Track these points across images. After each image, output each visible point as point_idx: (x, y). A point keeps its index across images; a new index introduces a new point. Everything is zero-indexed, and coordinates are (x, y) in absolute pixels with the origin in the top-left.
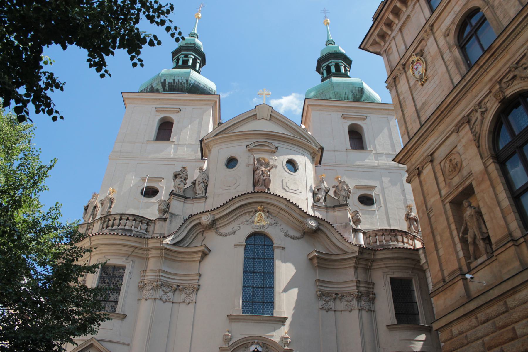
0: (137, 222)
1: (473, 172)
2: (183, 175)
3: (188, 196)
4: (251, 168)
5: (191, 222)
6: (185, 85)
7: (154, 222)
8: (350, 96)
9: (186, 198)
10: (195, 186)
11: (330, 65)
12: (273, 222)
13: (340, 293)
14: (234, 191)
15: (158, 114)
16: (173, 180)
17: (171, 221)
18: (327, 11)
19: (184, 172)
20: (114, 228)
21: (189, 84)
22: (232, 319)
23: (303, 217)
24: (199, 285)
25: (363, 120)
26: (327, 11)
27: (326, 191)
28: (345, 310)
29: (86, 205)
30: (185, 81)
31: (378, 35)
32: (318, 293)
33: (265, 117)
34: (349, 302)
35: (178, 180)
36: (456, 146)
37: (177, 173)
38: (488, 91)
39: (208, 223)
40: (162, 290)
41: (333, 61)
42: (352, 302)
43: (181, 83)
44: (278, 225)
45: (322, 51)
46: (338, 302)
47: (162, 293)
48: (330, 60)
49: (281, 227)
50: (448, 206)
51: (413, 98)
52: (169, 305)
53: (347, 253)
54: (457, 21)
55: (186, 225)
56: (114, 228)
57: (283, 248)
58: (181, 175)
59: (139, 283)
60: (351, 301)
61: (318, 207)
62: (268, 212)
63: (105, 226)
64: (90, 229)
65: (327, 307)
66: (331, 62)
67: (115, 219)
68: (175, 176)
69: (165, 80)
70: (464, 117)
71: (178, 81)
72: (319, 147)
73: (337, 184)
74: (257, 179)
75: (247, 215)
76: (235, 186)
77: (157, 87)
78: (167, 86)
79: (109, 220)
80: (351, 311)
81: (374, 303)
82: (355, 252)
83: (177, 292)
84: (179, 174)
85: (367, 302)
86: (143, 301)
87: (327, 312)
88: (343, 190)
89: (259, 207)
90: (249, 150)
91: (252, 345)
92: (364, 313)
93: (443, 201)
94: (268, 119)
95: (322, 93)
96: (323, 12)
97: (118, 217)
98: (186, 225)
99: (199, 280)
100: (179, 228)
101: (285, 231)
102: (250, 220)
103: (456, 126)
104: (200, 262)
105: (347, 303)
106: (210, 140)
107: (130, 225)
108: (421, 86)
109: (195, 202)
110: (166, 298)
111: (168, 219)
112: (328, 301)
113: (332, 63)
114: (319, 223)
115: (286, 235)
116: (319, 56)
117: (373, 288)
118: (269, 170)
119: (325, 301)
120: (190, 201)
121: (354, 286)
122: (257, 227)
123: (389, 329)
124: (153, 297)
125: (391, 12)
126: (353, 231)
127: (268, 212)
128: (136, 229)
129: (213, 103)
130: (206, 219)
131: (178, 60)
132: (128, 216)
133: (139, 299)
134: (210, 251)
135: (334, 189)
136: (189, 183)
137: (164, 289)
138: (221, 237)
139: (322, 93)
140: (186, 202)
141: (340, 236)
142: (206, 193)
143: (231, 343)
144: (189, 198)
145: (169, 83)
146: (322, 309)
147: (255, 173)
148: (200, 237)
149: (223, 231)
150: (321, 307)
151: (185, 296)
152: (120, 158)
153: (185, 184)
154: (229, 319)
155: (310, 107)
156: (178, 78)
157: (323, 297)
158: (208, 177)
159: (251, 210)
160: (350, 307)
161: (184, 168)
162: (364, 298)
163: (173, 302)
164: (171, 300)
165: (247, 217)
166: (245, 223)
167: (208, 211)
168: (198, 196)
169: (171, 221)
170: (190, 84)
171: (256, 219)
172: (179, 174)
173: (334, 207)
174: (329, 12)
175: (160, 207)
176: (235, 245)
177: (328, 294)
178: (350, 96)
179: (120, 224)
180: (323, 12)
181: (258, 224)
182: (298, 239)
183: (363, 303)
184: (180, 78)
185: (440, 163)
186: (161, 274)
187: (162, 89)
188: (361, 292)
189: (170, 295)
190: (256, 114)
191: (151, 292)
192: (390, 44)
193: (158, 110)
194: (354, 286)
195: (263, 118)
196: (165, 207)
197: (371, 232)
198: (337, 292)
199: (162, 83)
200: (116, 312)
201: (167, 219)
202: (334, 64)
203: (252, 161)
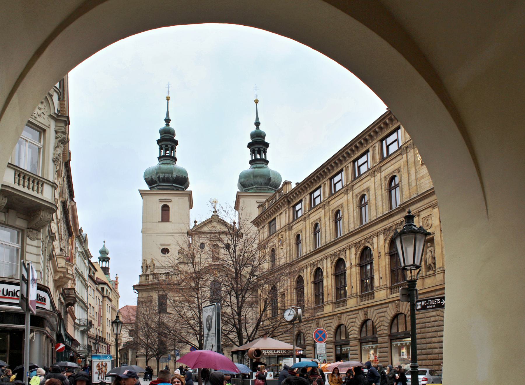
6: (171, 179)
8: (263, 183)
11: (255, 149)
15: (161, 203)
41: (257, 146)
43: (169, 178)
69: (159, 176)
77: (155, 179)
78: (161, 179)
113: (256, 147)
178: (263, 183)
193: (161, 201)
202: (257, 149)
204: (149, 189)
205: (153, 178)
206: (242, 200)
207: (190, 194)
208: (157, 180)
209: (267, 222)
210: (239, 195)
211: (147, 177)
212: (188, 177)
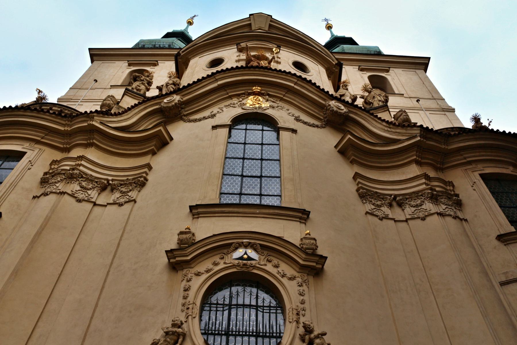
22: (198, 214)
23: (324, 100)
25: (386, 72)
39: (173, 104)
42: (423, 207)
44: (284, 109)
47: (78, 188)
48: (338, 45)
49: (289, 112)
60: (421, 205)
85: (449, 206)
89: (254, 88)
91: (236, 249)
98: (137, 110)
99: (147, 174)
102: (239, 103)
112: (380, 206)
119: (373, 204)
123: (502, 242)
133: (34, 197)
134: (172, 139)
141: (384, 124)
146: (372, 214)
156: (159, 43)
163: (95, 204)
164: (93, 200)
166: (231, 105)
183: (444, 207)
186: (83, 162)
191: (57, 185)
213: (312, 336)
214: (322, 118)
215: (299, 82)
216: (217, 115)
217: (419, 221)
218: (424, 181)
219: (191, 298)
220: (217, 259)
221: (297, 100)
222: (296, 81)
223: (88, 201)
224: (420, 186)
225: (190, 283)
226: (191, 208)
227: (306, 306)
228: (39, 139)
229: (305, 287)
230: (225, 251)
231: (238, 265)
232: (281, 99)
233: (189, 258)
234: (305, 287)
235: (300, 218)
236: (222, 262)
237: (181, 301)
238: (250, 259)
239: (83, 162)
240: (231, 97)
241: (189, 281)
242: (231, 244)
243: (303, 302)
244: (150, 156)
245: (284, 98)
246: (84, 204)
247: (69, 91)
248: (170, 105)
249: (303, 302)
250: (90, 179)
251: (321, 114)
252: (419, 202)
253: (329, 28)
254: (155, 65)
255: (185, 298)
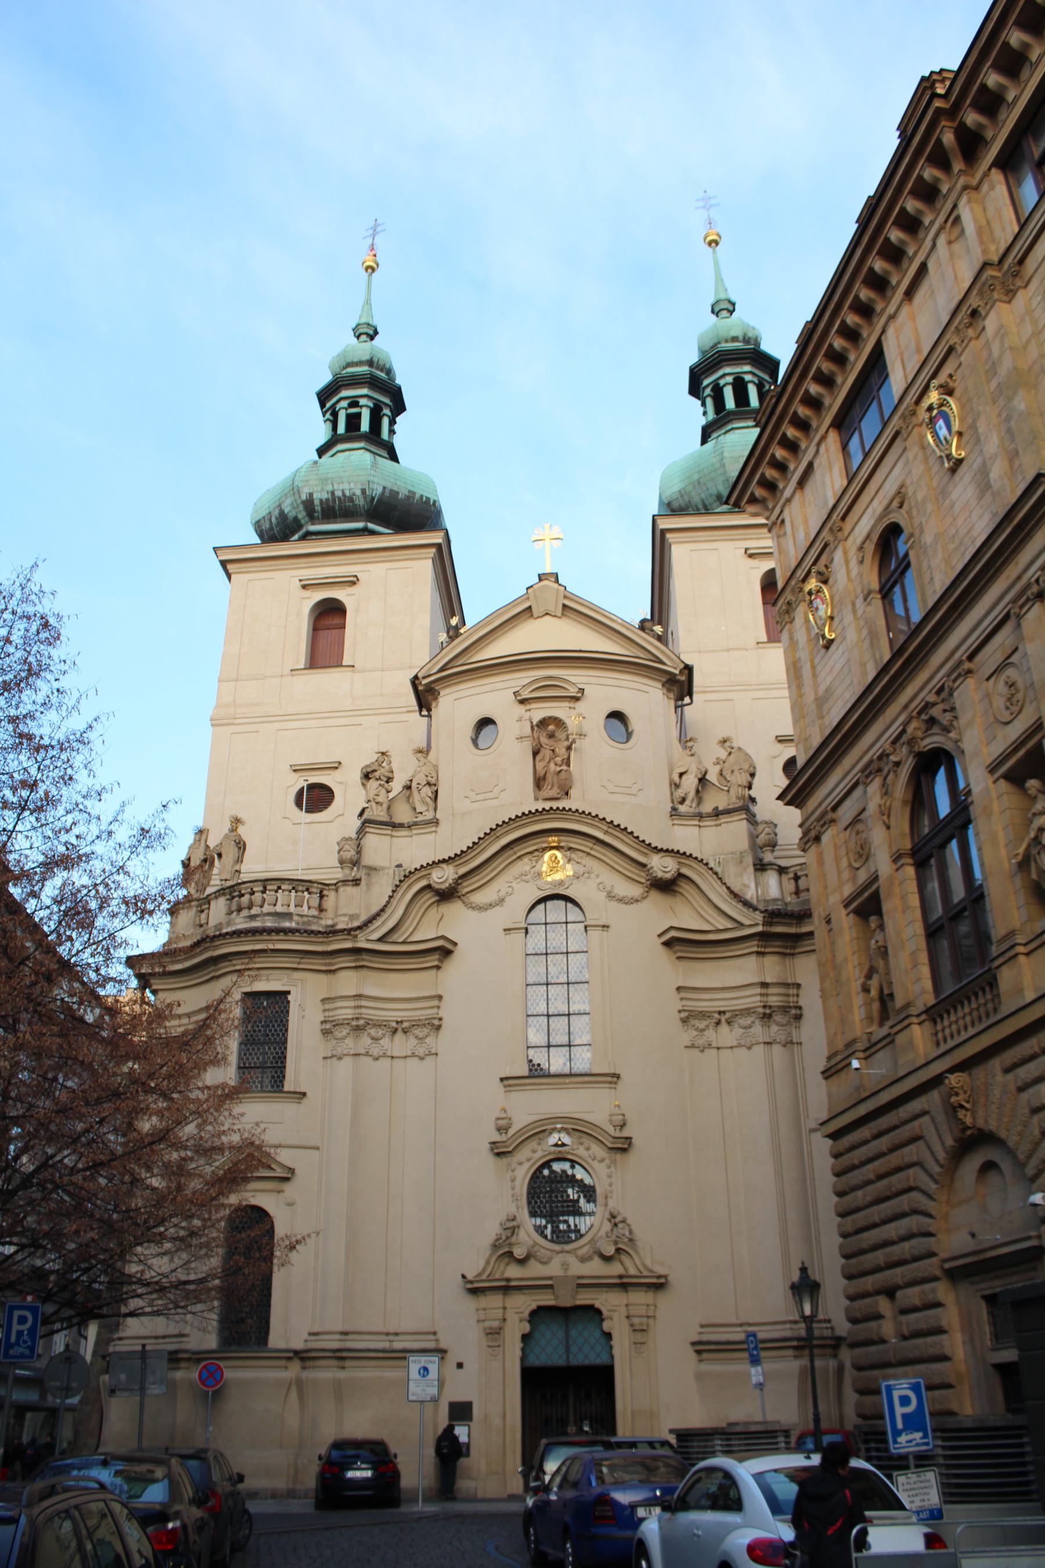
0: (300, 894)
1: (880, 873)
2: (382, 770)
3: (397, 820)
4: (527, 747)
5: (410, 886)
6: (360, 502)
7: (336, 886)
9: (395, 826)
10: (411, 793)
11: (722, 382)
12: (581, 869)
13: (729, 1011)
14: (495, 802)
15: (307, 593)
16: (363, 784)
17: (368, 885)
18: (712, 202)
19: (384, 764)
20: (254, 911)
21: (369, 499)
22: (510, 1086)
24: (440, 1019)
26: (712, 202)
27: (700, 776)
28: (739, 1046)
29: (183, 857)
30: (358, 492)
31: (759, 483)
32: (684, 1015)
33: (551, 609)
34: (745, 1028)
35: (373, 784)
36: (864, 809)
37: (369, 770)
38: (901, 728)
40: (369, 1034)
41: (728, 370)
42: (752, 1030)
43: (351, 499)
44: (592, 876)
45: (700, 340)
46: (724, 1028)
47: (370, 1041)
49: (599, 880)
50: (851, 916)
51: (813, 667)
52: (385, 1062)
53: (741, 925)
54: (875, 537)
55: (400, 894)
56: (254, 911)
57: (605, 927)
58: (377, 774)
59: (322, 1023)
60: (750, 1027)
61: (681, 816)
62: (570, 849)
63: (234, 907)
64: (202, 911)
65: (701, 1042)
66: (724, 376)
67: (253, 893)
68: (367, 776)
69: (311, 495)
70: (871, 762)
71: (344, 494)
72: (682, 666)
73: (723, 754)
74: (542, 774)
75: (526, 860)
76: (495, 790)
78: (318, 508)
79: (242, 895)
80: (749, 1048)
81: (798, 1027)
82: (757, 925)
83: (399, 1035)
84: (375, 771)
85: (783, 1026)
86: (335, 1059)
87: (702, 1051)
88: (736, 772)
90: (522, 702)
91: (551, 1133)
92: (776, 1048)
93: (846, 906)
94: (559, 614)
95: (699, 483)
96: (701, 204)
97: (258, 888)
98: (400, 894)
99: (438, 1007)
100: (388, 902)
101: (608, 888)
102: (532, 871)
103: (863, 771)
104: (438, 968)
105: (742, 1031)
106: (432, 678)
107: (285, 902)
108: (823, 651)
109: (414, 832)
110: (377, 1050)
111: (363, 883)
112: (702, 1030)
113: (726, 375)
114: (679, 863)
115: (610, 896)
116: (694, 358)
117: (798, 995)
118: (569, 748)
119: (696, 1029)
120: (404, 832)
121: (755, 995)
122: (548, 887)
124: (352, 1052)
125: (779, 443)
126: (756, 870)
127: (570, 849)
128: (299, 910)
129: (434, 550)
130: (442, 877)
131: (335, 414)
132: (278, 883)
133: (325, 1058)
134: (455, 944)
135: (718, 768)
136: (397, 786)
137: (373, 1032)
138: (474, 914)
139: (699, 483)
140: (395, 833)
141: (724, 888)
142: (435, 810)
143: (511, 1132)
144: (401, 826)
145: (321, 500)
146: (693, 1046)
147: (538, 758)
148: (433, 914)
149: (478, 898)
150: (689, 1044)
151: (413, 1042)
152: (237, 721)
153: (388, 792)
154: (505, 1086)
155: (668, 536)
156: (341, 487)
157: (693, 1022)
158: (436, 767)
159: (535, 848)
160: (748, 1040)
161: (383, 754)
162: (778, 1018)
164: (389, 1054)
165: (524, 865)
167: (444, 861)
168: (421, 818)
169: (368, 885)
170: (373, 498)
171: (545, 868)
172: (375, 771)
173: (717, 813)
174: (718, 205)
175: (342, 853)
176: (505, 930)
177: (703, 1015)
179: (264, 900)
180: (701, 204)
181: (549, 879)
182: (637, 901)
183: (774, 1028)
184: (346, 486)
185: (846, 829)
187: (307, 519)
188: (770, 1007)
189: (385, 1042)
190: (530, 608)
191: (346, 1041)
192: (782, 512)
194: (755, 995)
195: (547, 614)
196: (353, 853)
197: (798, 868)
198: (722, 1009)
199: (303, 502)
200: (286, 1088)
201: (360, 880)
202: (729, 379)
203: (528, 731)
204: (259, 541)
205: (286, 511)
206: (679, 553)
207: (439, 546)
208: (302, 515)
209: (828, 420)
210: (663, 532)
211: (264, 513)
212: (435, 502)
213: (617, 1220)
214: (643, 881)
215: (610, 830)
216: (507, 899)
217: (744, 1049)
218: (758, 990)
219: (517, 1189)
220: (533, 1144)
221: (609, 854)
222: (606, 828)
223: (384, 1055)
224: (752, 999)
225: (515, 1173)
226: (502, 1080)
227: (614, 1187)
228: (295, 966)
229: (613, 1169)
230: (541, 1136)
231: (554, 1152)
232: (588, 854)
233: (510, 1149)
234: (613, 1169)
235: (610, 1083)
236: (539, 1148)
237: (511, 1192)
238: (563, 1145)
239: (363, 1003)
240: (519, 857)
241: (513, 1171)
242: (545, 1131)
243: (611, 1185)
244: (434, 971)
245: (593, 852)
246: (381, 1059)
247: (219, 687)
248: (443, 887)
249: (611, 1185)
250: (378, 1025)
251: (643, 874)
252: (749, 1022)
253: (713, 245)
254: (353, 582)
255: (513, 1189)
